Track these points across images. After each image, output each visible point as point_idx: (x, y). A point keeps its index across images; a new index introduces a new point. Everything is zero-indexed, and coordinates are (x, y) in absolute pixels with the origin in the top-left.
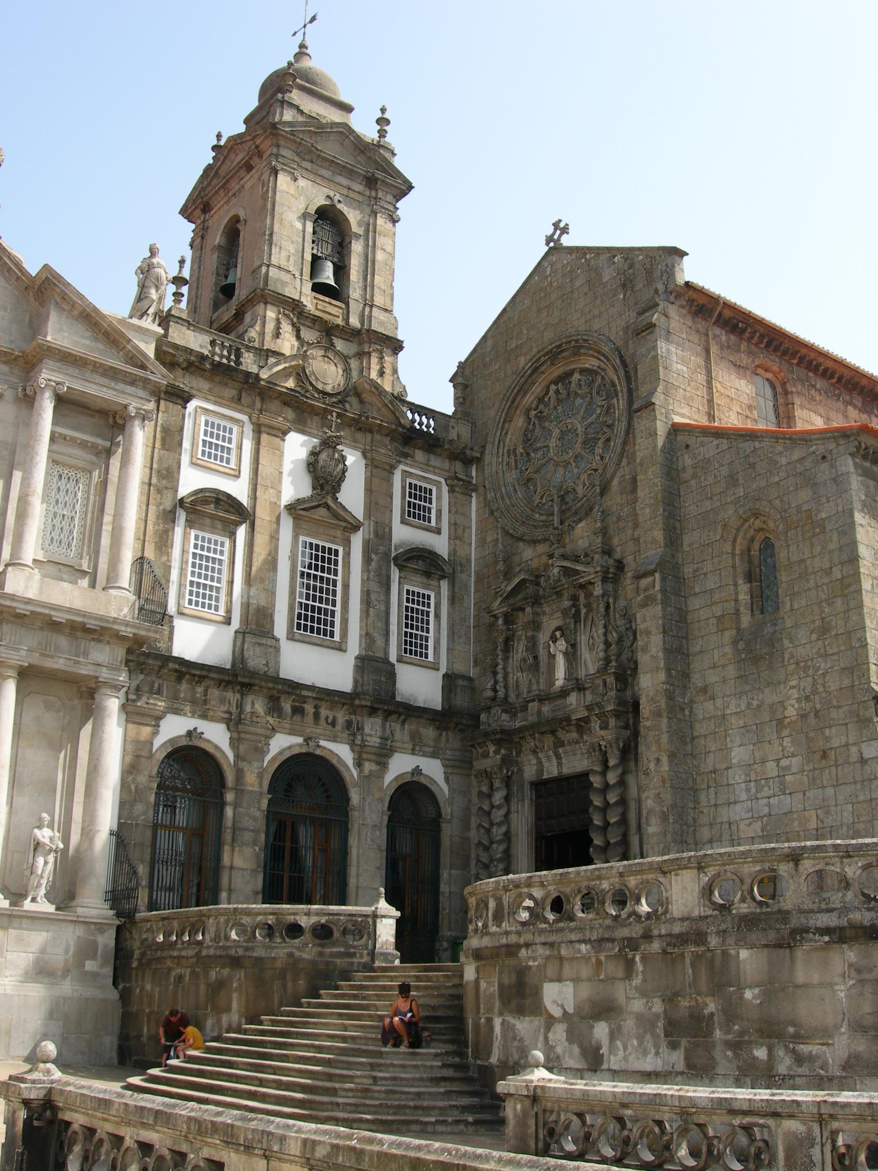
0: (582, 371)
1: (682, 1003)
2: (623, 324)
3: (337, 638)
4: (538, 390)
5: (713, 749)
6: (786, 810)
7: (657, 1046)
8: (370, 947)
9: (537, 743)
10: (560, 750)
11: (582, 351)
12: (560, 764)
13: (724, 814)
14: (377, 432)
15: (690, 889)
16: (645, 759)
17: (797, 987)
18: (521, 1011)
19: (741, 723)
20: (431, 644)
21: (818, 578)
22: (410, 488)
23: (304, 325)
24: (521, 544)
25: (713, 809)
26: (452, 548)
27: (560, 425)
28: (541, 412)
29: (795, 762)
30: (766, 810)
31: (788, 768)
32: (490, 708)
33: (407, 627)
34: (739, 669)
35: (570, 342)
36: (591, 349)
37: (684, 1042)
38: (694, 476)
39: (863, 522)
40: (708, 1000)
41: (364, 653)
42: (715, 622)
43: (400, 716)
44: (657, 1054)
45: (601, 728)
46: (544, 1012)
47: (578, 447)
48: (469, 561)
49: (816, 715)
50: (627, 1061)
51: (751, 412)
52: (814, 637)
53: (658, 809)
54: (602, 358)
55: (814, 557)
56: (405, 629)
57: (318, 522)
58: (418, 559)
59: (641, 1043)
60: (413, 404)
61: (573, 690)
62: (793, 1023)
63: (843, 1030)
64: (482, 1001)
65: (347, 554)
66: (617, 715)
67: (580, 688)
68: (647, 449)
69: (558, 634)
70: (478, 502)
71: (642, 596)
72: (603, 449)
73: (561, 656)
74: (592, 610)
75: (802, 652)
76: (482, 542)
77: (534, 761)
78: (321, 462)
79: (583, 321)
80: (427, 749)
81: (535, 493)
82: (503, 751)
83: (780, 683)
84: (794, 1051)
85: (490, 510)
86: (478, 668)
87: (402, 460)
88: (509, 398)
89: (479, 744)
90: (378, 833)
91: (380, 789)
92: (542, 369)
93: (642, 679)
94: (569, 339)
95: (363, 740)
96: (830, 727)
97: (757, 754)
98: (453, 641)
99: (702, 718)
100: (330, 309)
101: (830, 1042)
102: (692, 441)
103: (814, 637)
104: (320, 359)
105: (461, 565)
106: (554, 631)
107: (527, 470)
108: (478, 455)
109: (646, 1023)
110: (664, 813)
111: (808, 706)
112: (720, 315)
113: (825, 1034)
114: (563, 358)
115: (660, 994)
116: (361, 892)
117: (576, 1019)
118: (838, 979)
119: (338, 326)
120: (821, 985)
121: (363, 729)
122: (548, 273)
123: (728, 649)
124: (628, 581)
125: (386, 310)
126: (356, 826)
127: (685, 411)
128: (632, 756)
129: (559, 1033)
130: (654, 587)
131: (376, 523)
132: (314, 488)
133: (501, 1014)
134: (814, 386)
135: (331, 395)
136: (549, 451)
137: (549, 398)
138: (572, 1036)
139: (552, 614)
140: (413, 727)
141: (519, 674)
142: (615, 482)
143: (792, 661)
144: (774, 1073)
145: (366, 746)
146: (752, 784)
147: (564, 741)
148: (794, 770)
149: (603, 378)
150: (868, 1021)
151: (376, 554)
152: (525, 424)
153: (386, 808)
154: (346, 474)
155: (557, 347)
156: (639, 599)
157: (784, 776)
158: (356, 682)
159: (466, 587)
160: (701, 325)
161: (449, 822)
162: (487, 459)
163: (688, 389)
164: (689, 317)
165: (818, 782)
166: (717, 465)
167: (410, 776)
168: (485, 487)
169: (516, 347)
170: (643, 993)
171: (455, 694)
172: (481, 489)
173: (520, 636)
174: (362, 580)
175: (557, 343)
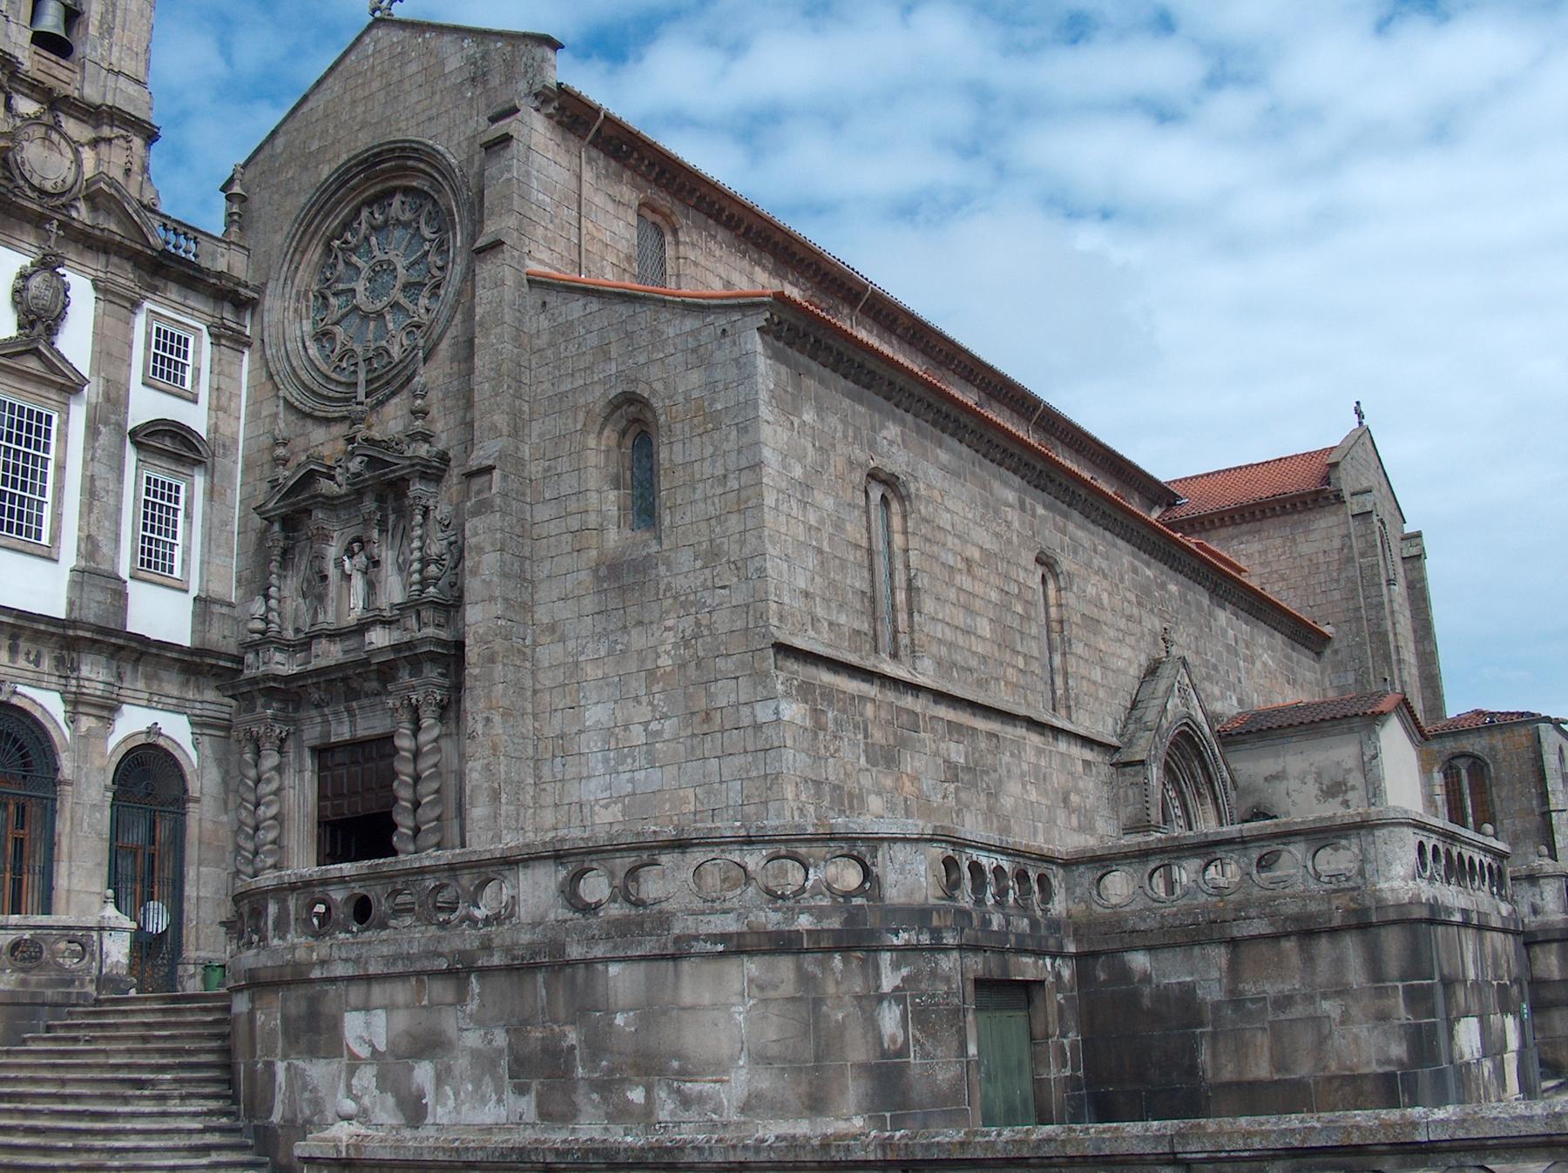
0: (407, 191)
1: (533, 1034)
2: (469, 132)
3: (45, 540)
5: (561, 706)
6: (655, 788)
7: (499, 1091)
8: (95, 972)
10: (354, 704)
11: (410, 163)
12: (353, 723)
13: (575, 792)
14: (116, 254)
15: (543, 885)
16: (470, 718)
17: (683, 1009)
18: (313, 1053)
19: (600, 674)
20: (178, 552)
21: (708, 487)
22: (158, 335)
23: (18, 92)
24: (309, 423)
25: (559, 785)
26: (212, 422)
28: (346, 242)
29: (669, 726)
30: (629, 788)
31: (659, 733)
33: (145, 529)
34: (599, 603)
35: (393, 150)
36: (422, 161)
37: (535, 1085)
38: (551, 344)
39: (771, 419)
40: (567, 1028)
41: (83, 563)
42: (570, 540)
44: (500, 1101)
46: (345, 1052)
48: (236, 441)
49: (698, 665)
50: (458, 1113)
51: (631, 265)
52: (699, 564)
53: (486, 785)
55: (703, 459)
56: (142, 532)
57: (25, 376)
58: (164, 436)
59: (477, 1086)
60: (168, 218)
62: (677, 1055)
63: (741, 1063)
64: (258, 1040)
65: (65, 422)
66: (433, 658)
68: (491, 302)
69: (356, 546)
70: (251, 361)
71: (473, 500)
73: (359, 575)
75: (680, 583)
76: (254, 416)
77: (319, 719)
78: (33, 291)
79: (413, 122)
80: (169, 701)
82: (274, 705)
83: (652, 623)
84: (678, 1091)
85: (269, 375)
87: (149, 295)
88: (303, 220)
90: (98, 815)
91: (103, 755)
93: (467, 614)
95: (78, 686)
96: (716, 680)
97: (619, 715)
98: (209, 552)
99: (547, 665)
100: (57, 71)
101: (726, 1078)
102: (553, 299)
103: (699, 564)
104: (38, 142)
105: (224, 446)
106: (351, 543)
107: (322, 320)
108: (256, 296)
109: (484, 1062)
110: (494, 790)
111: (687, 654)
112: (598, 130)
113: (718, 1069)
114: (383, 171)
115: (502, 1023)
116: (74, 899)
117: (390, 1059)
118: (734, 999)
119: (67, 97)
120: (714, 1006)
121: (79, 669)
122: (370, 52)
123: (585, 576)
125: (138, 82)
126: (68, 806)
127: (545, 255)
128: (452, 714)
129: (366, 1077)
130: (490, 488)
131: (108, 381)
132: (20, 327)
133: (285, 1057)
134: (714, 237)
135: (52, 195)
136: (354, 297)
137: (360, 224)
138: (383, 1082)
139: (348, 521)
141: (300, 600)
142: (444, 345)
143: (668, 594)
144: (653, 1120)
145: (83, 694)
146: (612, 755)
148: (666, 736)
150: (774, 1050)
151: (106, 424)
153: (109, 781)
154: (69, 309)
156: (468, 504)
157: (654, 743)
158: (71, 604)
159: (230, 475)
160: (573, 143)
161: (197, 801)
162: (267, 303)
163: (551, 226)
164: (559, 130)
165: (698, 753)
166: (583, 332)
167: (144, 736)
170: (480, 1022)
171: (210, 624)
172: (257, 344)
174: (85, 461)
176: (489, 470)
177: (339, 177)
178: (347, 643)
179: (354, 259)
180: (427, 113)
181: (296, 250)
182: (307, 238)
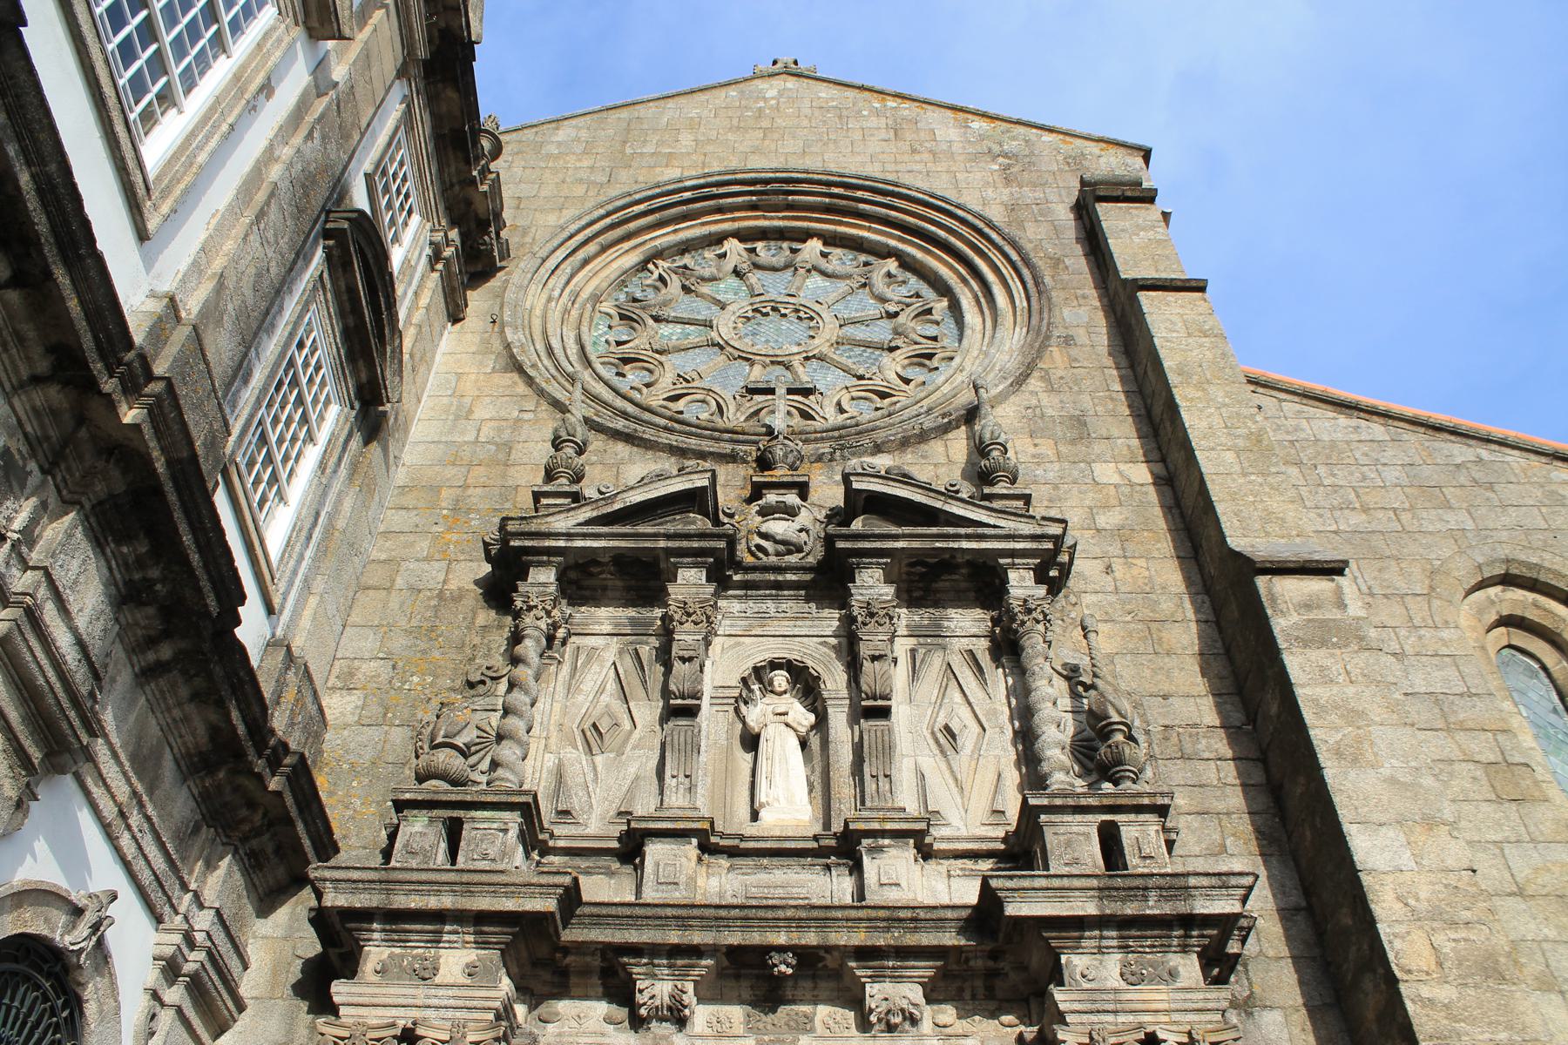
2: (1005, 198)
11: (862, 206)
24: (622, 449)
28: (685, 267)
35: (829, 184)
43: (166, 635)
54: (933, 228)
69: (780, 679)
72: (904, 367)
73: (795, 743)
86: (355, 699)
130: (1342, 605)
137: (724, 255)
140: (154, 730)
141: (575, 757)
176: (1333, 570)
182: (619, 232)
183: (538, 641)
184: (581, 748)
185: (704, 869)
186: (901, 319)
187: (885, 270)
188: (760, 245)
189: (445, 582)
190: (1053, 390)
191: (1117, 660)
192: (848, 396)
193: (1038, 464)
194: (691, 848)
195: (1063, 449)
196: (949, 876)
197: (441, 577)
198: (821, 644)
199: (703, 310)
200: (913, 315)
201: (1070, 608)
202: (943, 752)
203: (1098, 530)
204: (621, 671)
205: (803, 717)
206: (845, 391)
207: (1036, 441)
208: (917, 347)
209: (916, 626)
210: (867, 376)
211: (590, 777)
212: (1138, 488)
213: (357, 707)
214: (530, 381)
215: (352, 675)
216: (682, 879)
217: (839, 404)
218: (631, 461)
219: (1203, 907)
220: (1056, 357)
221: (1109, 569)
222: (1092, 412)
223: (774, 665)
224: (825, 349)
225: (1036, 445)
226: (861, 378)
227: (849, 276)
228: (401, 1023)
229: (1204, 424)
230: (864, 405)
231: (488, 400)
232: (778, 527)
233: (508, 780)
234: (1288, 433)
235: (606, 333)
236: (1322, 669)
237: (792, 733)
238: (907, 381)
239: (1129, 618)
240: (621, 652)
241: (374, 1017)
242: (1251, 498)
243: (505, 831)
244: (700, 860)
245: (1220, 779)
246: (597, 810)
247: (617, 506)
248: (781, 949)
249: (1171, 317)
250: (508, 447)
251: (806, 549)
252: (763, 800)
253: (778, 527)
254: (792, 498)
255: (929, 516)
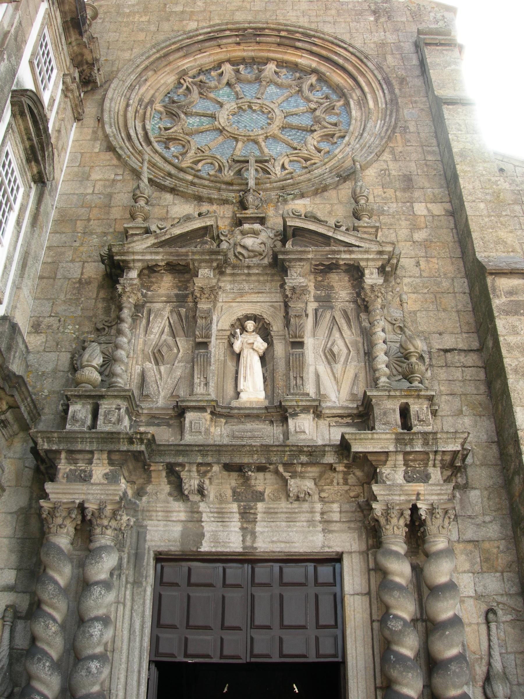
0: (281, 64)
2: (376, 39)
4: (207, 60)
9: (207, 482)
10: (260, 506)
24: (169, 197)
27: (240, 101)
28: (201, 81)
32: (102, 397)
35: (279, 31)
45: (408, 479)
47: (274, 129)
61: (305, 410)
67: (318, 414)
69: (250, 325)
71: (504, 299)
74: (332, 308)
77: (183, 516)
81: (184, 154)
88: (163, 48)
89: (70, 452)
92: (225, 41)
94: (281, 27)
124: (405, 289)
139: (242, 295)
141: (150, 366)
147: (262, 494)
149: (322, 78)
152: (171, 86)
155: (255, 29)
168: (100, 120)
169: (182, 12)
172: (89, 120)
173: (159, 310)
175: (260, 25)
177: (209, 33)
178: (235, 428)
179: (212, 95)
180: (319, 19)
181: (146, 68)
183: (130, 309)
184: (153, 362)
185: (213, 423)
186: (318, 113)
187: (309, 82)
188: (241, 67)
189: (82, 274)
190: (396, 160)
191: (418, 314)
192: (288, 160)
193: (385, 203)
194: (207, 416)
195: (398, 194)
196: (330, 426)
197: (79, 272)
198: (271, 306)
199: (210, 107)
200: (324, 110)
201: (397, 285)
202: (329, 363)
203: (414, 242)
204: (172, 322)
205: (261, 345)
206: (286, 157)
207: (385, 190)
208: (325, 130)
209: (318, 297)
210: (298, 148)
211: (158, 377)
212: (436, 218)
213: (43, 342)
214: (119, 157)
215: (39, 325)
216: (203, 429)
217: (283, 165)
218: (175, 204)
219: (443, 447)
220: (398, 144)
221: (418, 264)
222: (415, 173)
223: (247, 318)
224: (277, 132)
225: (385, 193)
226: (295, 149)
227: (290, 86)
228: (78, 501)
229: (471, 187)
230: (297, 165)
231: (97, 168)
232: (249, 241)
233: (120, 383)
234: (517, 185)
235: (158, 123)
236: (514, 327)
237: (256, 354)
238: (319, 151)
239: (426, 291)
240: (171, 312)
241: (65, 499)
242: (491, 230)
243: (119, 409)
244: (212, 420)
245: (463, 377)
246: (162, 394)
247: (167, 237)
248: (249, 465)
249: (459, 121)
250: (110, 196)
251: (264, 254)
252: (242, 388)
253: (249, 241)
254: (257, 226)
255: (326, 240)
